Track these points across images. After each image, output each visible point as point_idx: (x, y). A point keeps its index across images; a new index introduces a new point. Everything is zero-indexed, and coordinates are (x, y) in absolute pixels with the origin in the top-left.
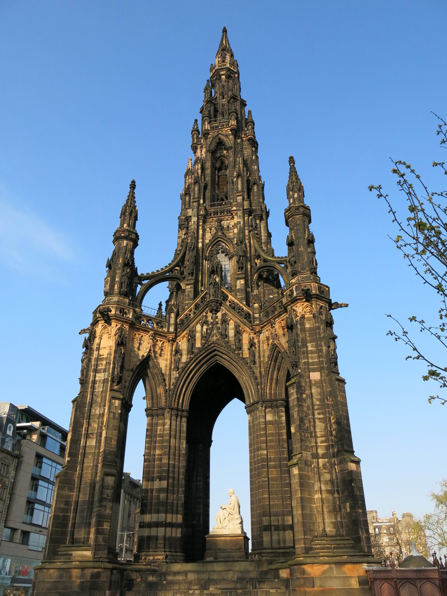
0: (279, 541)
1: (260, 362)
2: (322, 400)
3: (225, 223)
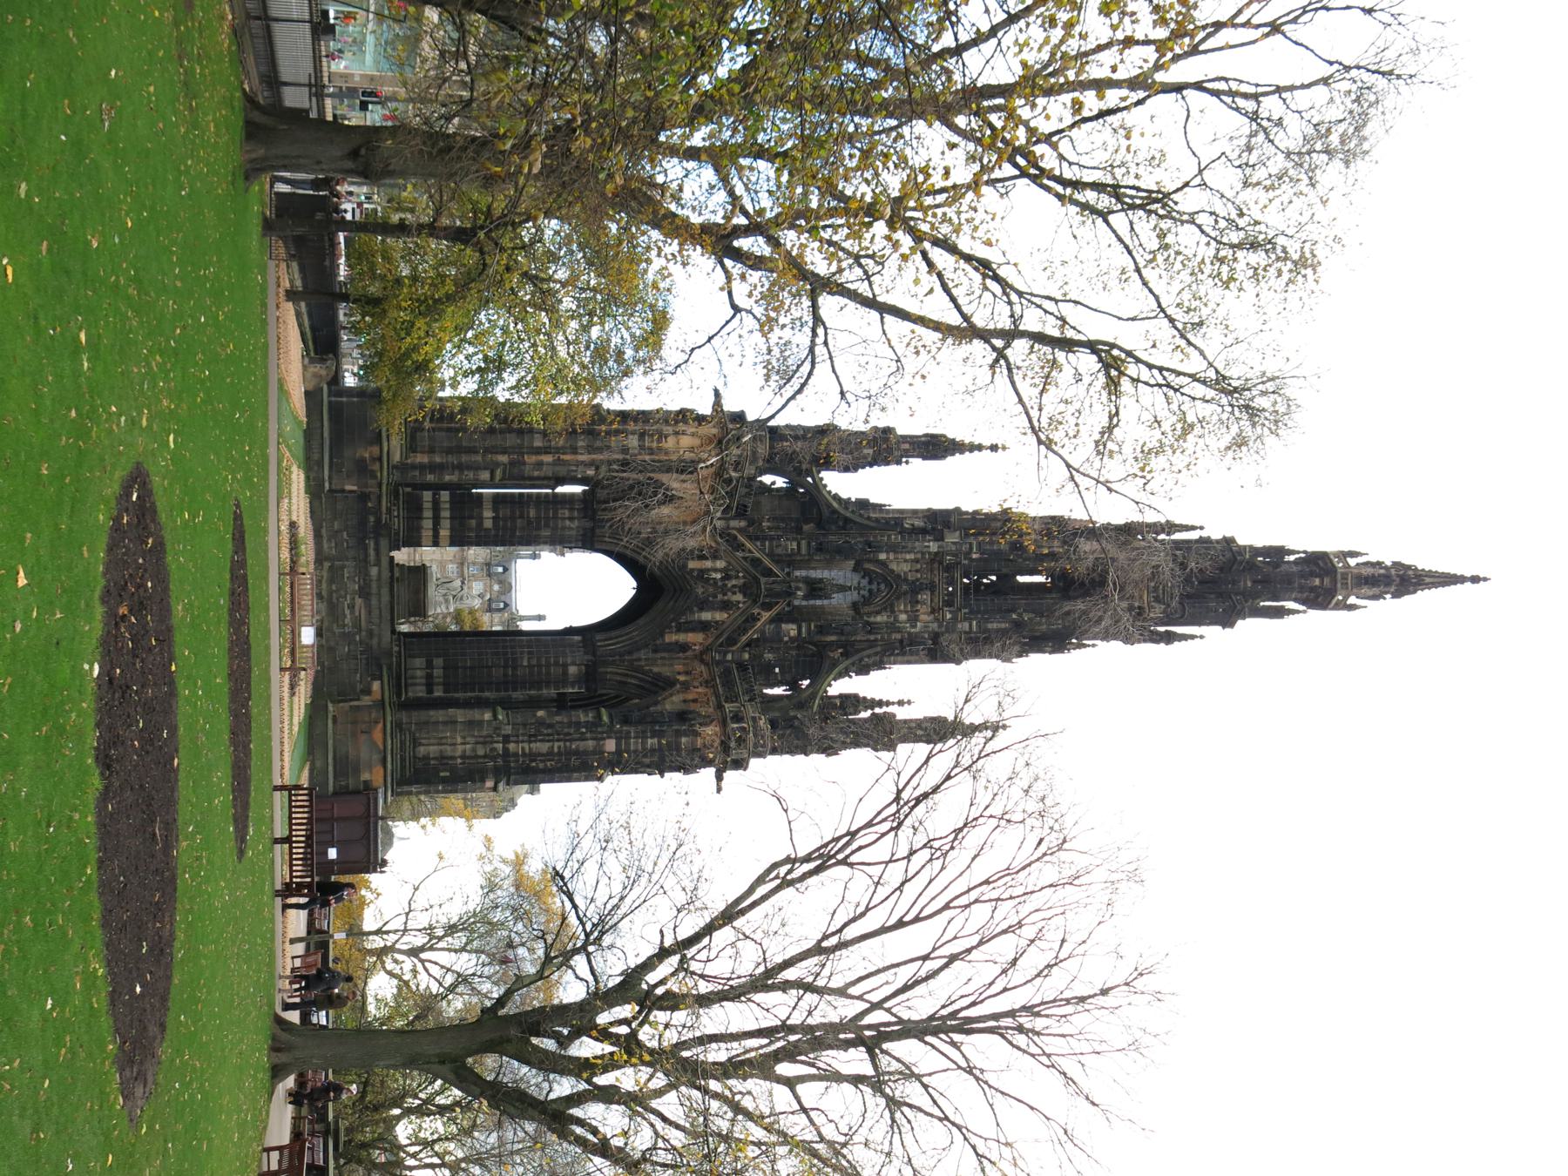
0: (413, 677)
2: (577, 752)
3: (925, 596)
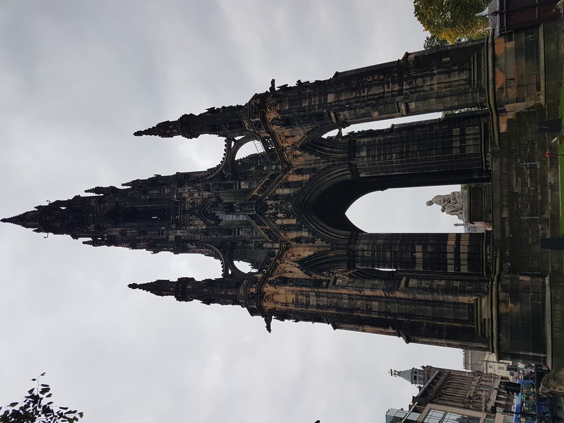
1: (315, 163)
2: (352, 90)
3: (188, 207)
